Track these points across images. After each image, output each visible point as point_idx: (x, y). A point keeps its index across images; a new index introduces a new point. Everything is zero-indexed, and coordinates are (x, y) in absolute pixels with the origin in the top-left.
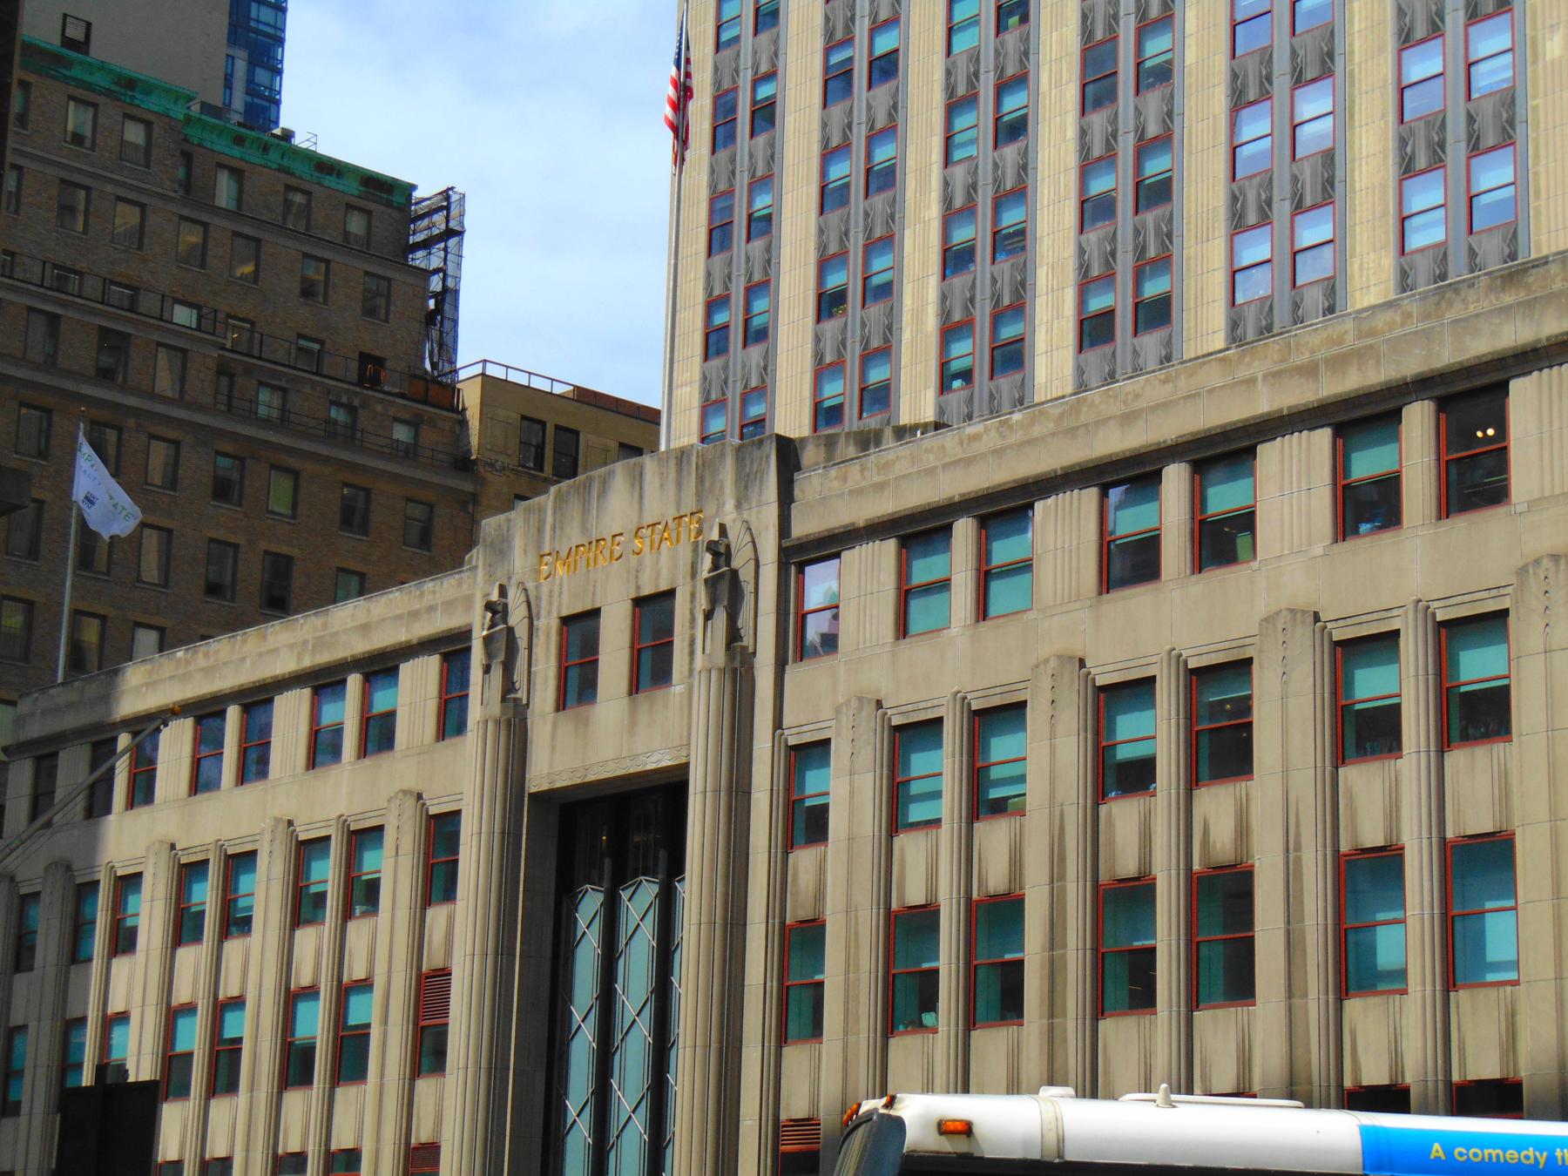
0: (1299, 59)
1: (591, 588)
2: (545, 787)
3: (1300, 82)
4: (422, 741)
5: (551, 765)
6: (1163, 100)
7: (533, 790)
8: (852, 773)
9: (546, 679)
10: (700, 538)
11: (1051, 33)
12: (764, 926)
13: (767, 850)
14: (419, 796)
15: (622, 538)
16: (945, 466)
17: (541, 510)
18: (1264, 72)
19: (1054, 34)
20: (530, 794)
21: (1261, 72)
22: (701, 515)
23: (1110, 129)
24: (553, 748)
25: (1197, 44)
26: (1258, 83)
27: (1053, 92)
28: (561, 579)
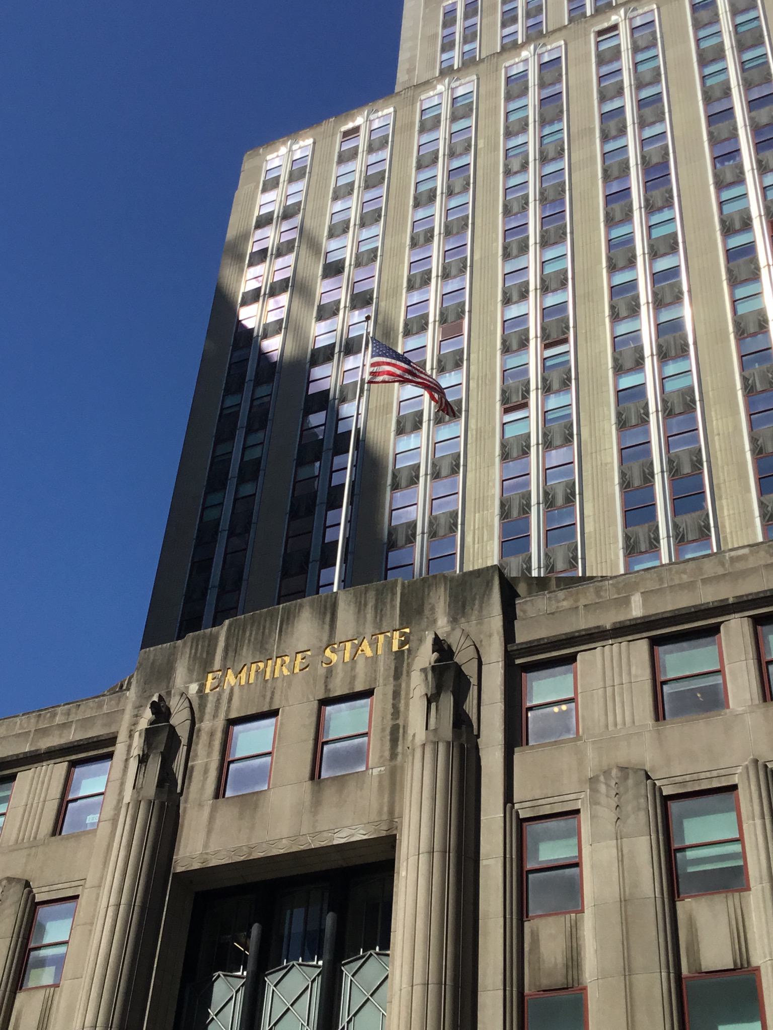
0: (681, 530)
1: (268, 695)
2: (196, 866)
3: (683, 541)
4: (35, 838)
5: (206, 846)
6: (569, 550)
7: (179, 869)
8: (619, 837)
9: (206, 771)
10: (407, 647)
11: (475, 513)
12: (500, 993)
13: (502, 914)
14: (27, 884)
15: (309, 653)
16: (704, 581)
17: (214, 639)
18: (652, 536)
19: (477, 515)
20: (175, 874)
21: (649, 536)
22: (407, 630)
23: (525, 566)
24: (209, 832)
25: (595, 521)
26: (647, 542)
27: (476, 546)
28: (232, 689)
